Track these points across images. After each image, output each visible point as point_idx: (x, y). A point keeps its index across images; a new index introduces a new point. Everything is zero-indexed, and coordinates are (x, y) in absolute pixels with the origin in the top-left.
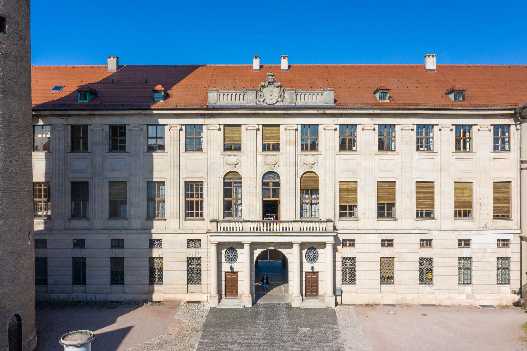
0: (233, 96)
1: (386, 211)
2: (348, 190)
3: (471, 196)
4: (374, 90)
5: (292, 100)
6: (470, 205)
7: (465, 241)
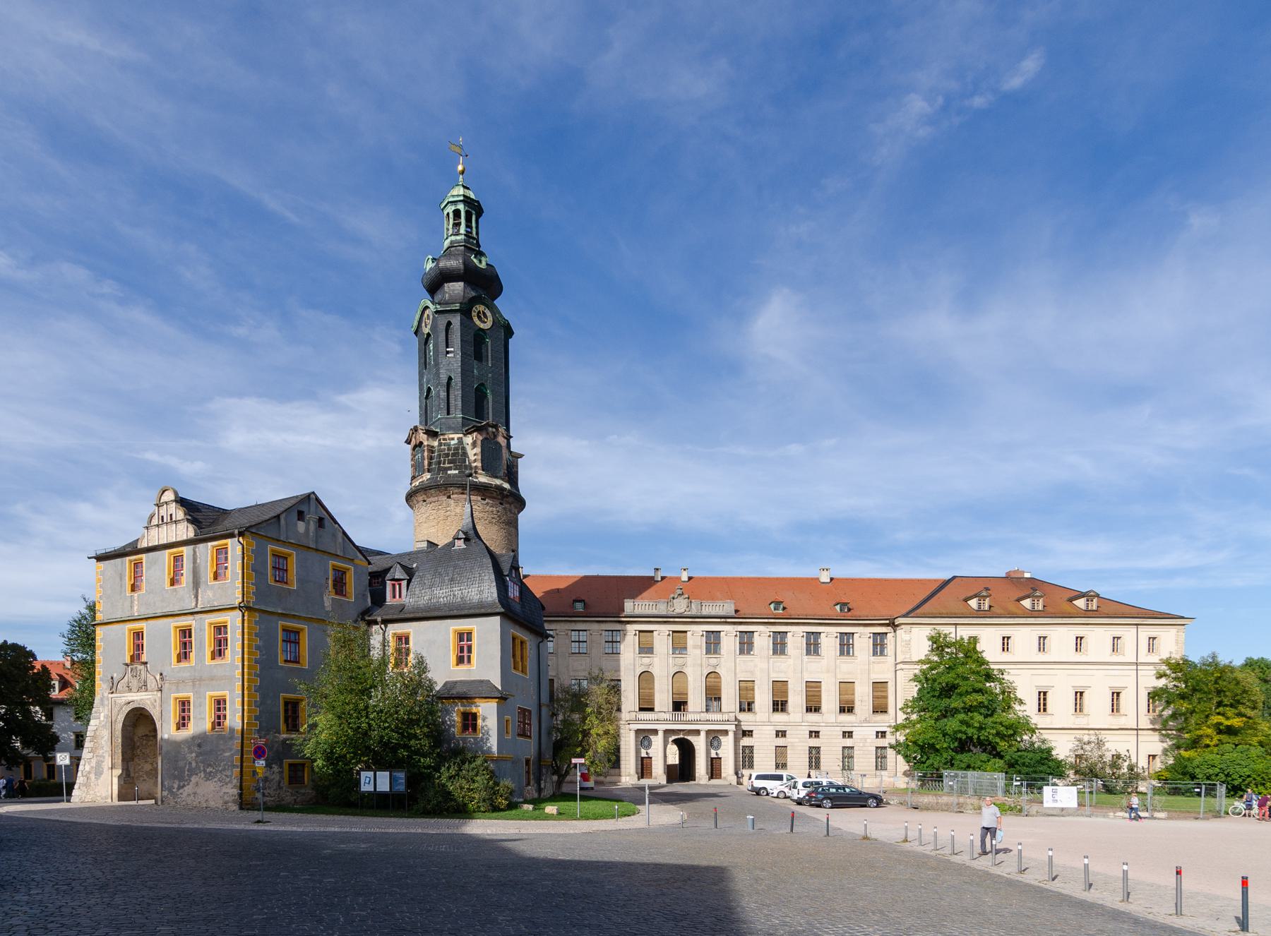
0: (647, 606)
1: (780, 707)
2: (747, 689)
3: (853, 694)
4: (769, 603)
5: (698, 610)
6: (853, 702)
7: (849, 732)
